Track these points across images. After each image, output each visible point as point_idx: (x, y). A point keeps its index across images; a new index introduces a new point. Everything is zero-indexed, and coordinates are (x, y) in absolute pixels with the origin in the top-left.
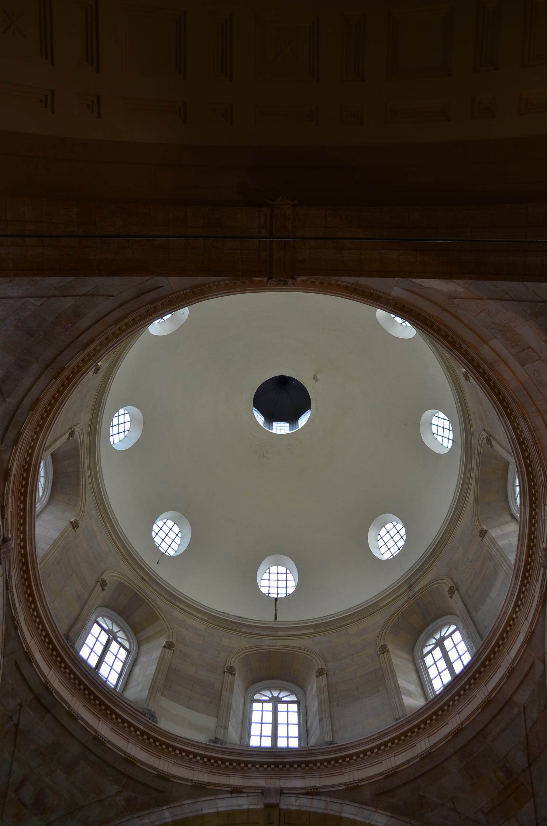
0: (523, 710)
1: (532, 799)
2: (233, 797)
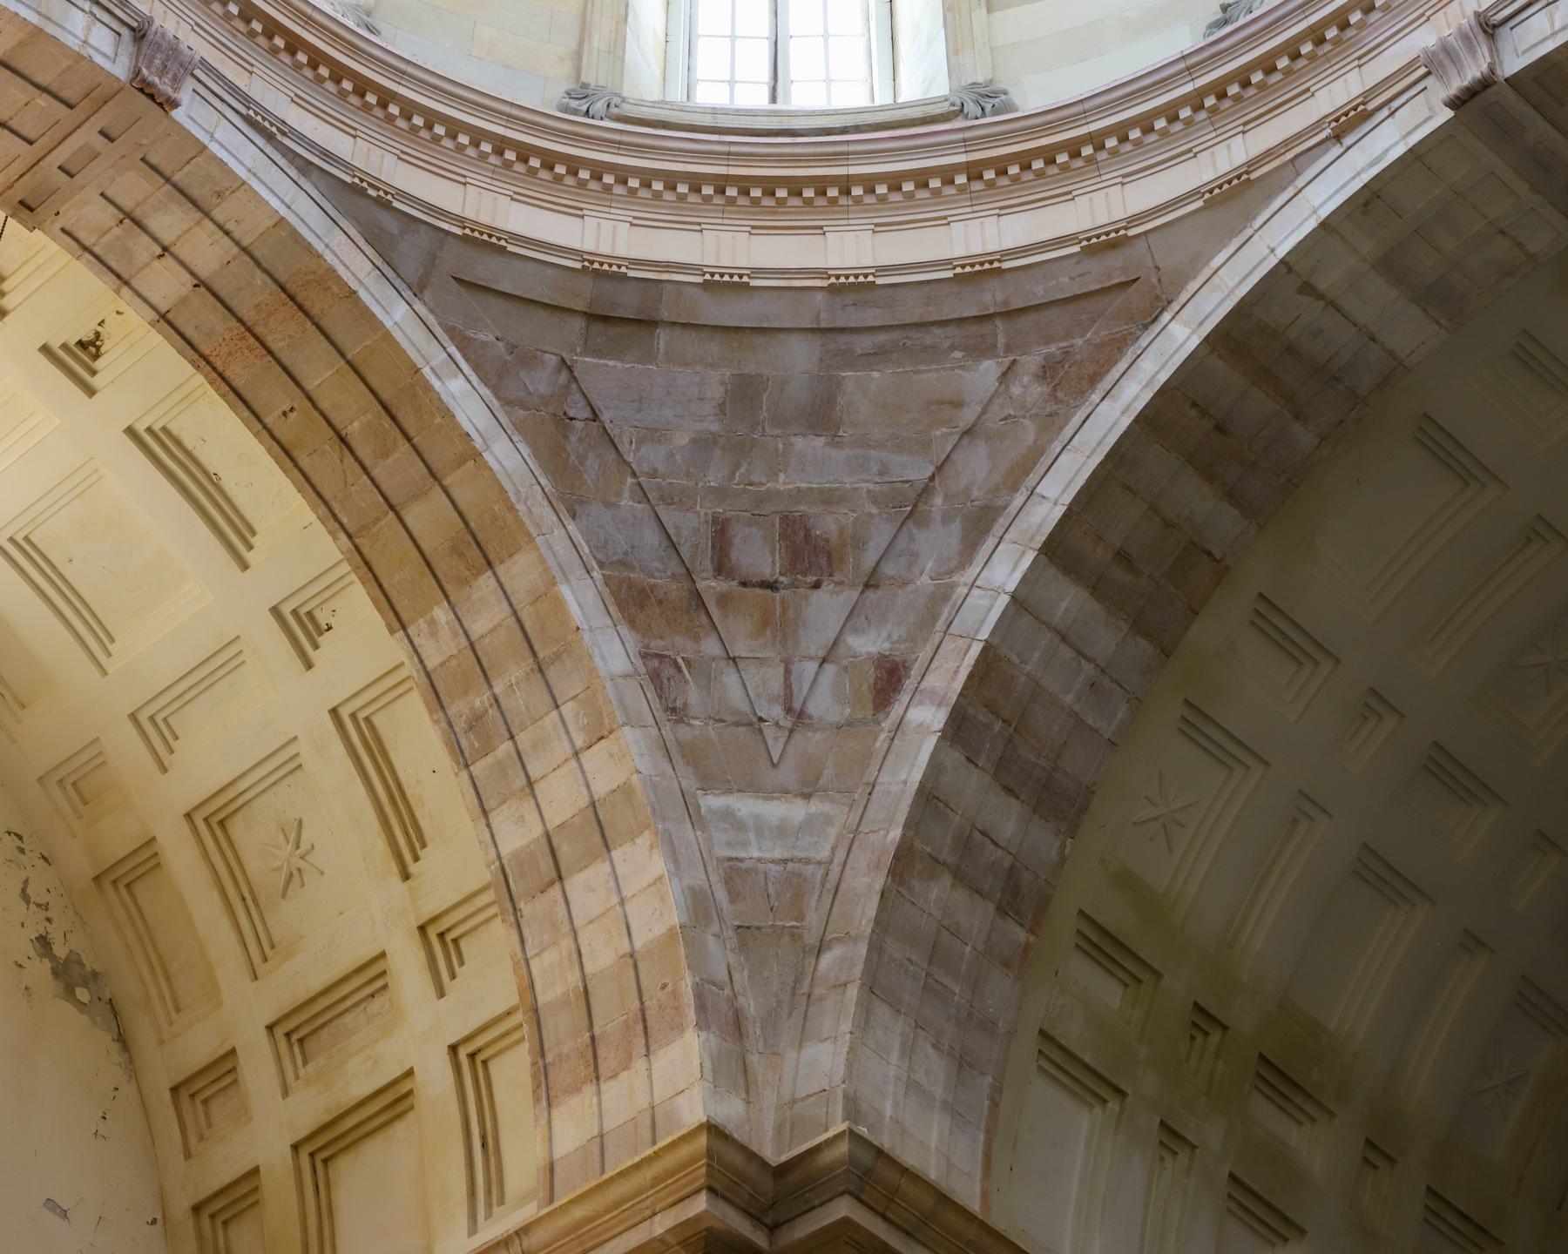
2: (1349, 148)
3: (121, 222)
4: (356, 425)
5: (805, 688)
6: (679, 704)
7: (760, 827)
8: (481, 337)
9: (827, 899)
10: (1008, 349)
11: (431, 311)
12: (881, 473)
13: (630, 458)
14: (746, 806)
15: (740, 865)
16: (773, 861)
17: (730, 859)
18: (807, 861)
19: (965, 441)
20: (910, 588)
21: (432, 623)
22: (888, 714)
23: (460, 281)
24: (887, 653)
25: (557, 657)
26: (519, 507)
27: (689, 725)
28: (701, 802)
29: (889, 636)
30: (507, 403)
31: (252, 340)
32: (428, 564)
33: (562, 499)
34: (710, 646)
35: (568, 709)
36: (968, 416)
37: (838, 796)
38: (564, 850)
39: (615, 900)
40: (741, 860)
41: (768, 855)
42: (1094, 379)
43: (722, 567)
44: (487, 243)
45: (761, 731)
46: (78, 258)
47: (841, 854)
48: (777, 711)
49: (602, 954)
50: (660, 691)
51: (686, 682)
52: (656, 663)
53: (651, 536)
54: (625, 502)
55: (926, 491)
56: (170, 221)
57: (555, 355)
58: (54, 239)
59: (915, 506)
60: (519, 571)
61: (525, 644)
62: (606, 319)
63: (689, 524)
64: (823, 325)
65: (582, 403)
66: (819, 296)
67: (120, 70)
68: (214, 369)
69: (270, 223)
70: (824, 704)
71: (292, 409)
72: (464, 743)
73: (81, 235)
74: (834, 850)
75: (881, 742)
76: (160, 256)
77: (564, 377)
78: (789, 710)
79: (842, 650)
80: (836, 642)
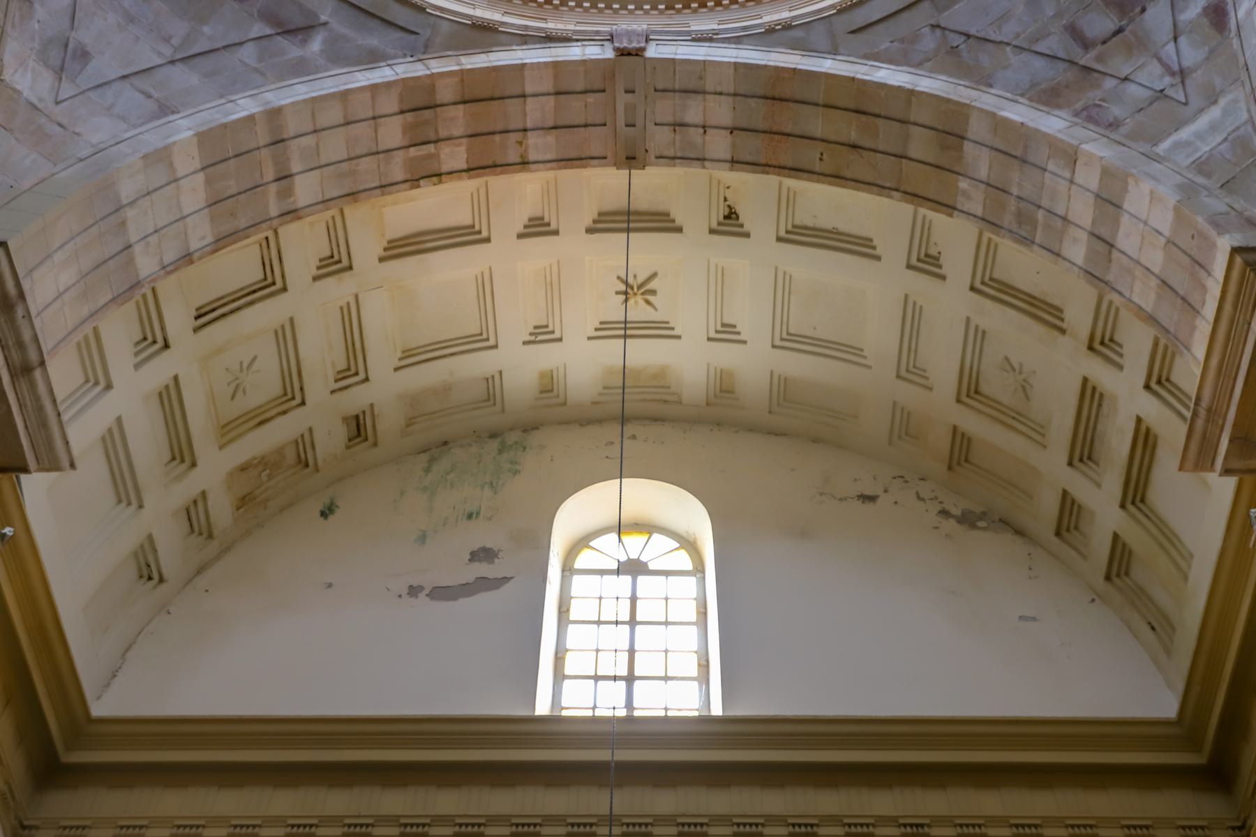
3: (675, 131)
5: (1175, 58)
6: (1111, 120)
7: (1200, 136)
8: (883, 47)
11: (849, 55)
13: (999, 39)
14: (1185, 134)
15: (1201, 160)
16: (1219, 144)
17: (1194, 162)
18: (1238, 128)
21: (965, 193)
23: (853, 32)
24: (1207, 5)
25: (1026, 147)
27: (1124, 124)
30: (918, 65)
31: (776, 136)
32: (938, 167)
33: (978, 82)
34: (1109, 83)
35: (1051, 167)
37: (1232, 87)
38: (1103, 232)
39: (1142, 225)
40: (1200, 157)
41: (1214, 144)
45: (1166, 96)
46: (674, 166)
48: (1168, 80)
49: (1155, 258)
50: (1097, 123)
51: (1108, 108)
52: (1085, 113)
53: (1039, 63)
56: (694, 112)
57: (926, 26)
58: (657, 165)
60: (977, 129)
61: (1007, 157)
63: (1055, 43)
65: (957, 36)
67: (609, 53)
68: (775, 167)
69: (732, 71)
70: (1190, 54)
71: (822, 154)
72: (1023, 234)
73: (666, 153)
75: (1235, 42)
76: (705, 132)
77: (938, 32)
78: (1173, 74)
79: (1181, 26)
80: (1175, 25)
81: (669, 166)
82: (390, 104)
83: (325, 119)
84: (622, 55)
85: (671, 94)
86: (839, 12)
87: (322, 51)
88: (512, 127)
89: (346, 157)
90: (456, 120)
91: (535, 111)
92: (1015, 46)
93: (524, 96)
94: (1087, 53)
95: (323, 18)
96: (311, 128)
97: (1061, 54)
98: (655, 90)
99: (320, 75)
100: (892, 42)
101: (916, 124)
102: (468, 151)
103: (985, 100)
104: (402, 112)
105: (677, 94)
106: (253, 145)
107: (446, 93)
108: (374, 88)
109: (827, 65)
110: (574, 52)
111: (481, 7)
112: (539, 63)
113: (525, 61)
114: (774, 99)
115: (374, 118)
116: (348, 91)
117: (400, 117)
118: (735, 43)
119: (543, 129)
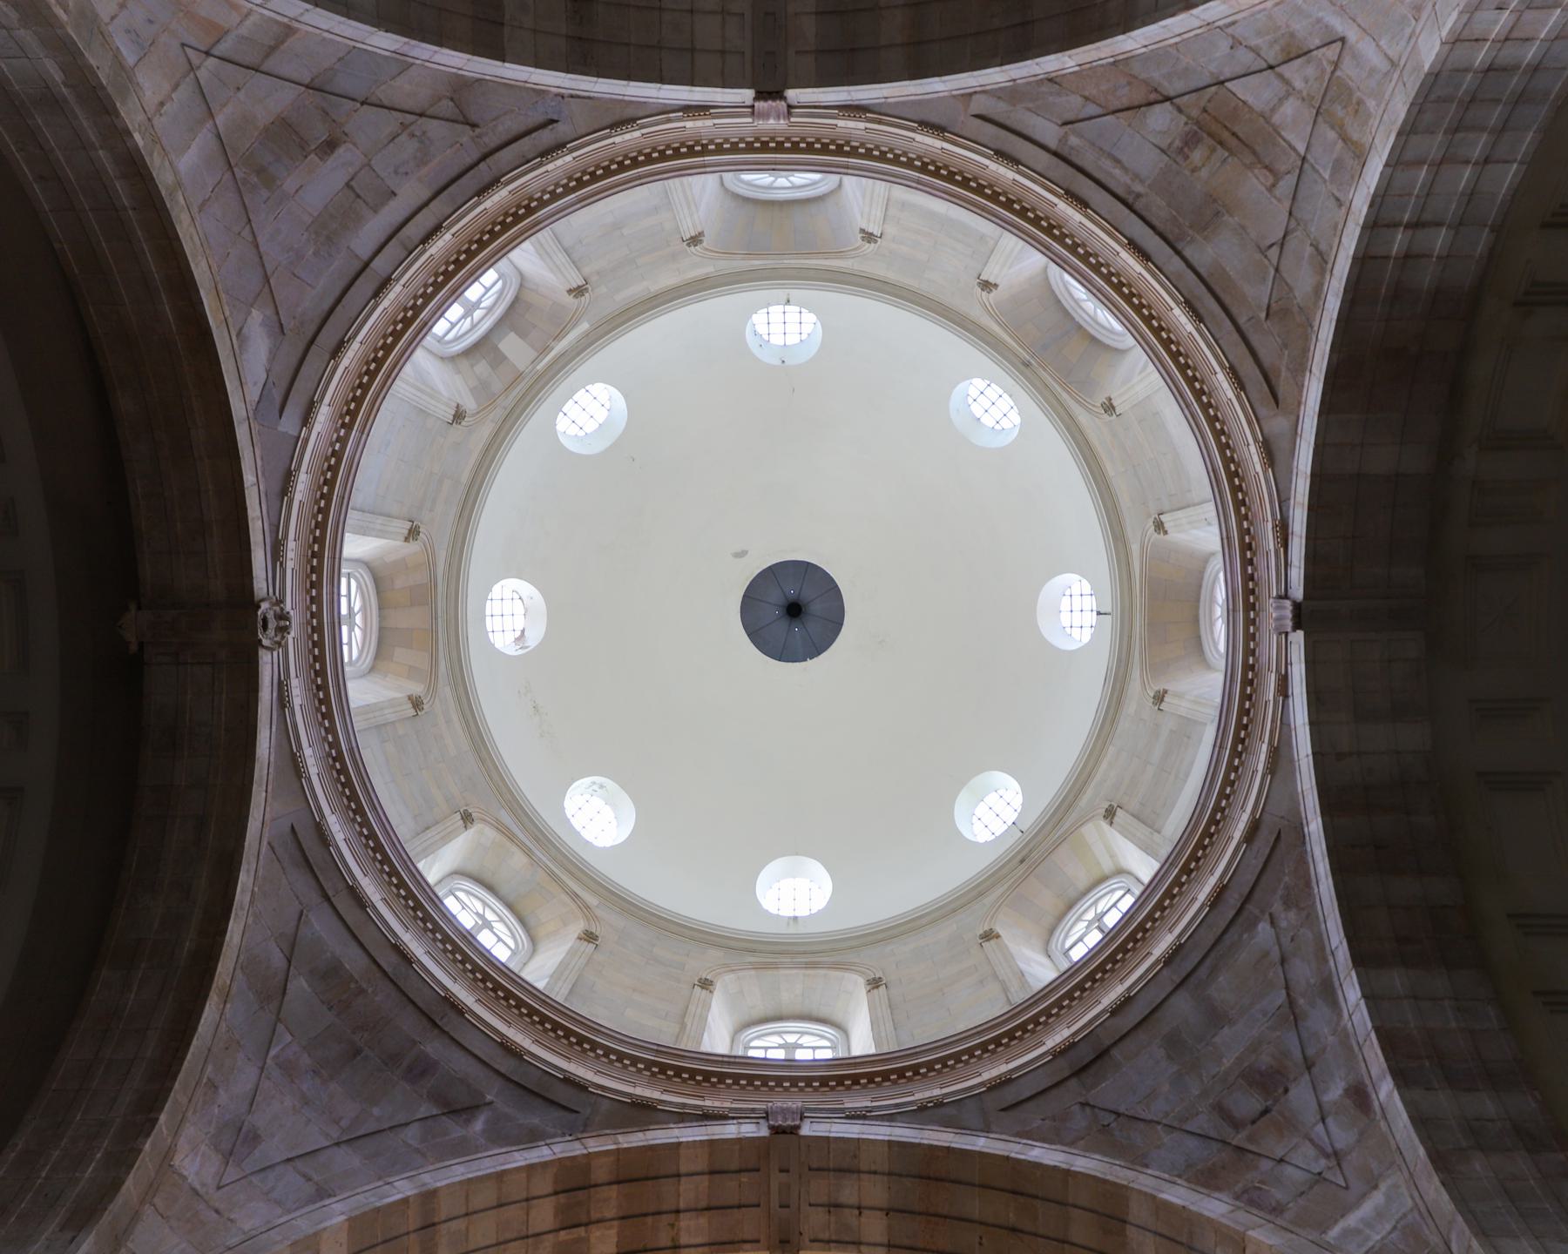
0: (1070, 126)
1: (1226, 84)
3: (829, 1212)
4: (1011, 1215)
5: (1326, 1139)
6: (1274, 1204)
7: (1368, 1223)
8: (1035, 1125)
9: (1430, 1221)
10: (1263, 912)
11: (1001, 1133)
12: (1265, 1015)
13: (1149, 1117)
16: (1390, 1233)
18: (1405, 1215)
19: (1286, 966)
20: (1329, 1048)
22: (1374, 1112)
23: (1003, 1110)
26: (1108, 1177)
28: (1328, 1239)
29: (1341, 1078)
30: (1072, 1144)
31: (933, 1219)
33: (1132, 1162)
34: (1266, 1165)
36: (1275, 955)
37: (1390, 1172)
40: (1373, 1247)
41: (1384, 1233)
42: (1308, 884)
43: (1237, 1125)
44: (1003, 1082)
46: (830, 1250)
47: (1416, 1194)
50: (1259, 1207)
51: (1268, 1191)
52: (1246, 1196)
53: (1192, 1143)
54: (1166, 1139)
55: (1291, 1002)
58: (811, 1249)
59: (1294, 1014)
60: (1138, 1212)
62: (1084, 1068)
63: (1203, 1122)
64: (1178, 981)
66: (1165, 972)
67: (764, 1132)
69: (886, 1149)
71: (981, 1238)
73: (821, 1236)
74: (1412, 1198)
75: (1383, 1124)
76: (860, 1213)
77: (1088, 1110)
81: (824, 1250)
82: (544, 1185)
83: (478, 1202)
84: (777, 1133)
85: (826, 1173)
86: (989, 1089)
87: (484, 1131)
88: (665, 1208)
89: (494, 1242)
90: (609, 1201)
91: (689, 1191)
92: (1165, 1125)
93: (679, 1175)
94: (1238, 1132)
95: (489, 1098)
96: (463, 1211)
97: (1213, 1134)
98: (810, 1169)
99: (479, 1155)
100: (1043, 1120)
101: (1075, 1206)
102: (619, 1234)
103: (1143, 1181)
104: (556, 1193)
105: (832, 1173)
106: (402, 1231)
107: (600, 1173)
108: (531, 1168)
109: (980, 1143)
110: (730, 1131)
111: (641, 1086)
112: (695, 1141)
113: (681, 1140)
114: (929, 1178)
115: (527, 1200)
116: (504, 1172)
117: (553, 1198)
118: (888, 1121)
119: (696, 1210)
